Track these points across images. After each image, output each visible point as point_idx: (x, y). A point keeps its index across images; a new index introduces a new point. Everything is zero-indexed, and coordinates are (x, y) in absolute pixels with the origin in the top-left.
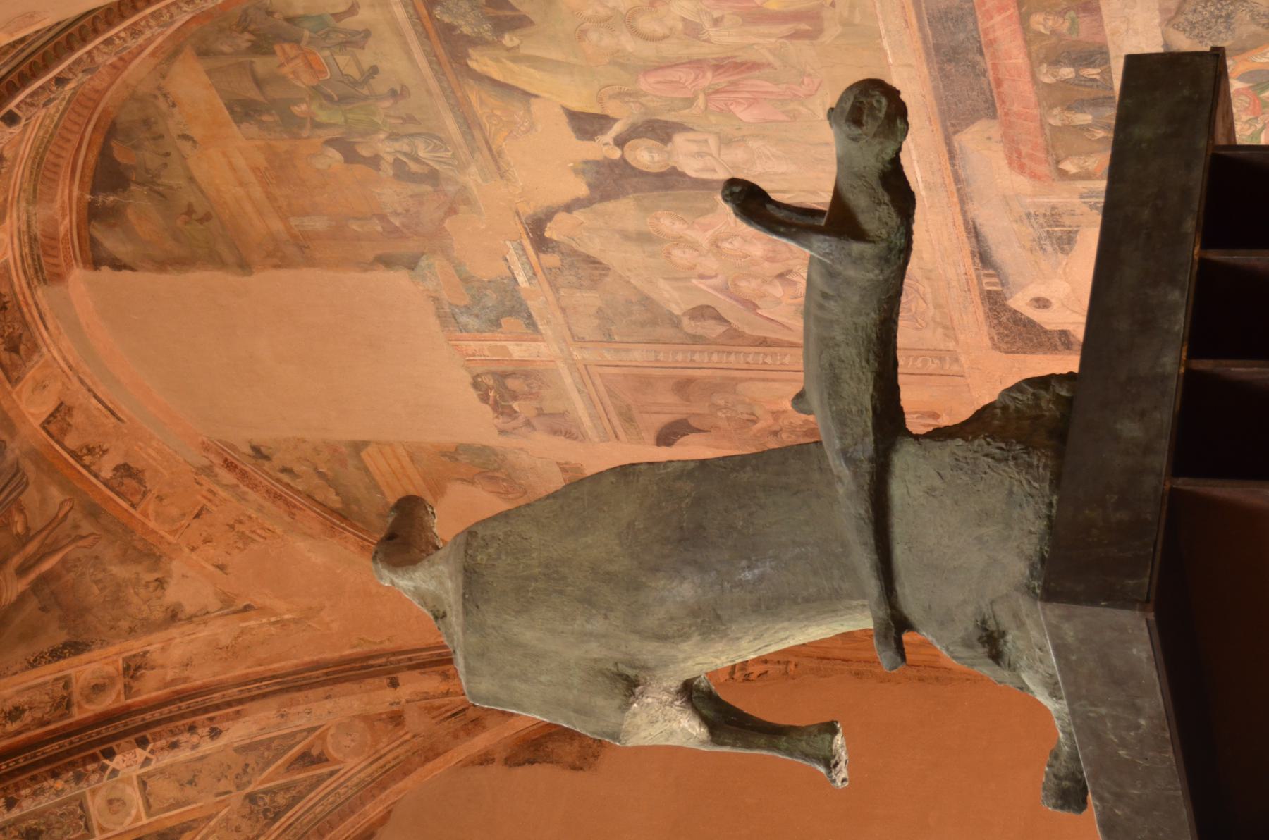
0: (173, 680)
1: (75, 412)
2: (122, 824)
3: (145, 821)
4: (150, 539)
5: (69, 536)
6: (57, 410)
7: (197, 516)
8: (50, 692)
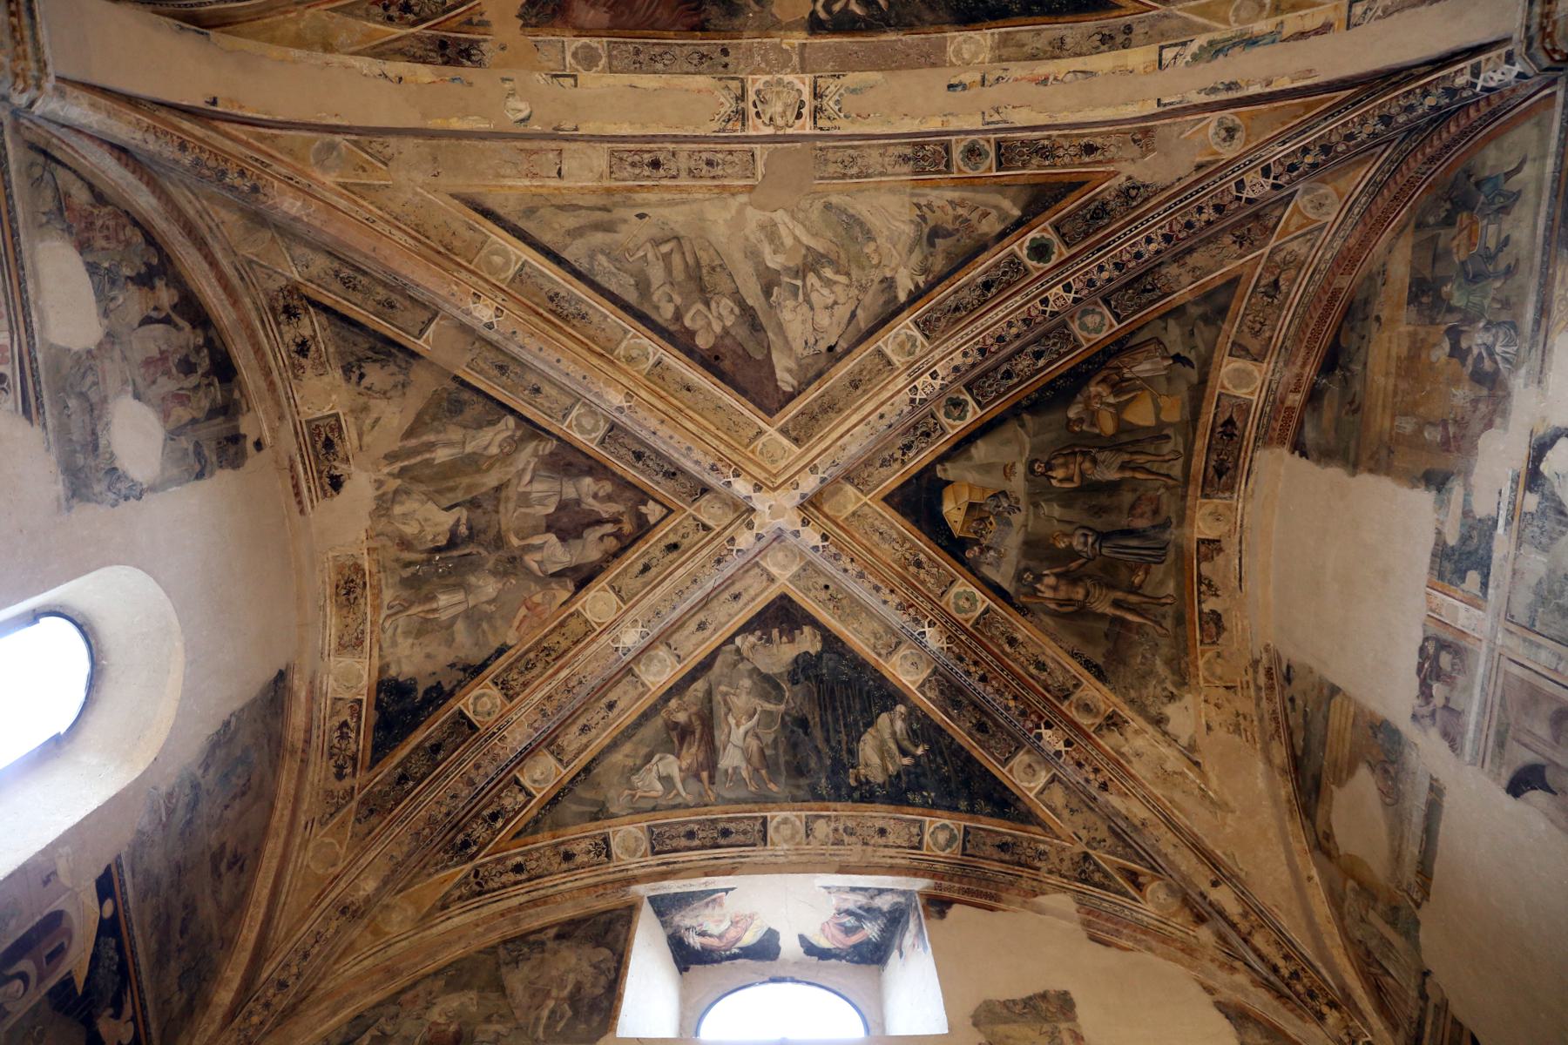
1: (1222, 554)
3: (1032, 795)
4: (1191, 669)
6: (1214, 541)
7: (1227, 688)
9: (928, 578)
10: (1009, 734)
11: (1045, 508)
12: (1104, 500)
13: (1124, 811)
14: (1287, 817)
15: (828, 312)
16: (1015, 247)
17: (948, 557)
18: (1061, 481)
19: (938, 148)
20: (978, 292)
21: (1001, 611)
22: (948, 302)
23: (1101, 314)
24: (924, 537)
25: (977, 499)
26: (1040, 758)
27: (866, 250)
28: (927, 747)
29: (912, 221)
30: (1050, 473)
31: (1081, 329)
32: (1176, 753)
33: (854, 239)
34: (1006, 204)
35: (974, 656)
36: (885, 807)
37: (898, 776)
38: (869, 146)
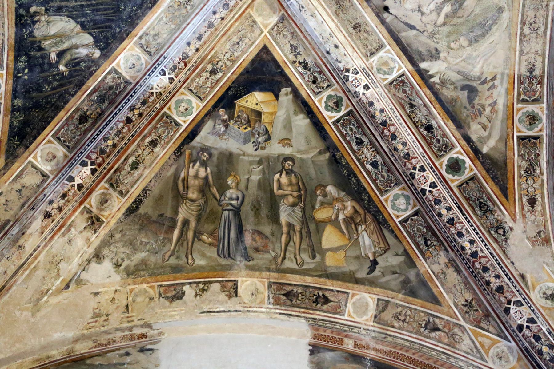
0: (70, 230)
1: (227, 298)
2: (41, 150)
3: (30, 158)
4: (140, 279)
5: (177, 252)
7: (127, 306)
8: (126, 185)
9: (203, 79)
10: (79, 141)
11: (258, 169)
12: (264, 212)
13: (29, 232)
14: (36, 357)
15: (416, 7)
16: (459, 148)
17: (219, 95)
18: (279, 180)
19: (538, 94)
20: (424, 121)
21: (178, 135)
22: (418, 100)
23: (407, 209)
24: (235, 77)
25: (265, 118)
26: (61, 166)
27: (462, 39)
28: (66, 74)
29: (482, 73)
30: (284, 172)
31: (394, 196)
32: (74, 271)
33: (472, 30)
34: (492, 143)
35: (146, 113)
36: (13, 36)
37: (41, 49)
38: (545, 43)
